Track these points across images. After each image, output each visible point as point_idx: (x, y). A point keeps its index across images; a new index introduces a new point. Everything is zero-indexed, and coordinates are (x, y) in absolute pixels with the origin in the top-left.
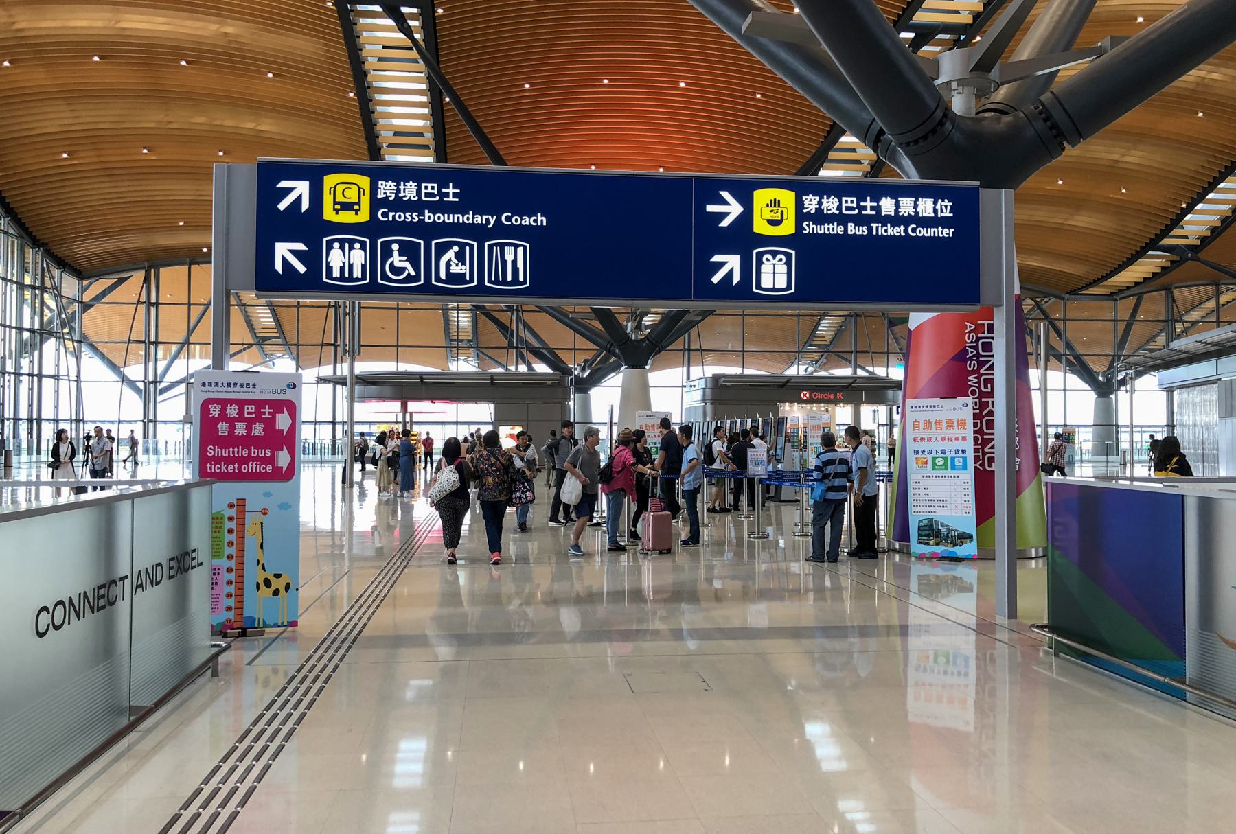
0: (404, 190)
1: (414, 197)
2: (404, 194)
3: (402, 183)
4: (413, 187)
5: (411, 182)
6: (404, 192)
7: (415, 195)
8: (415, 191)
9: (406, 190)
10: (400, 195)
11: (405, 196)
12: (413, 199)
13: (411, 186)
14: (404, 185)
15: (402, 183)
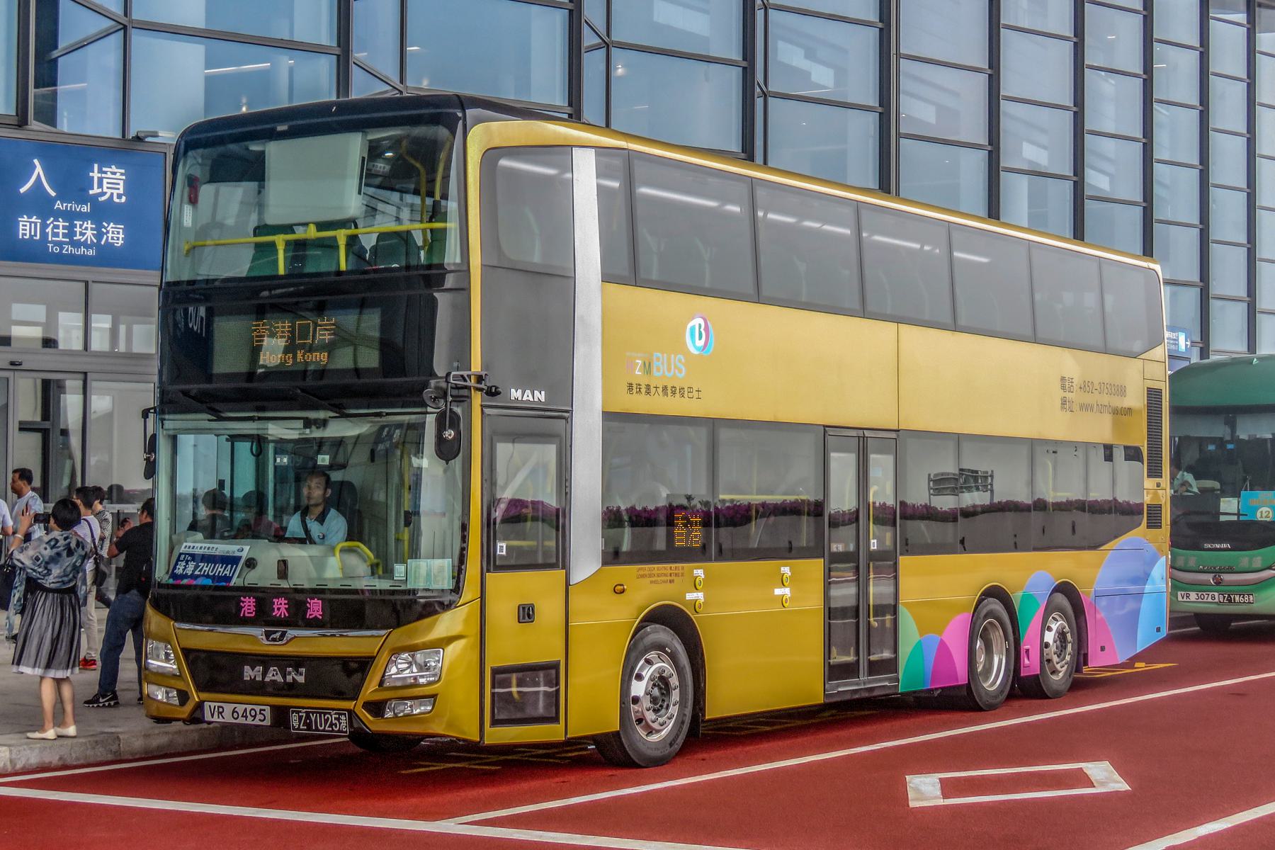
0: (100, 180)
1: (119, 196)
2: (100, 190)
3: (96, 166)
4: (118, 176)
5: (114, 169)
6: (100, 185)
7: (121, 191)
8: (121, 183)
9: (105, 181)
10: (91, 192)
11: (103, 194)
12: (116, 200)
13: (114, 173)
14: (100, 171)
15: (96, 166)
